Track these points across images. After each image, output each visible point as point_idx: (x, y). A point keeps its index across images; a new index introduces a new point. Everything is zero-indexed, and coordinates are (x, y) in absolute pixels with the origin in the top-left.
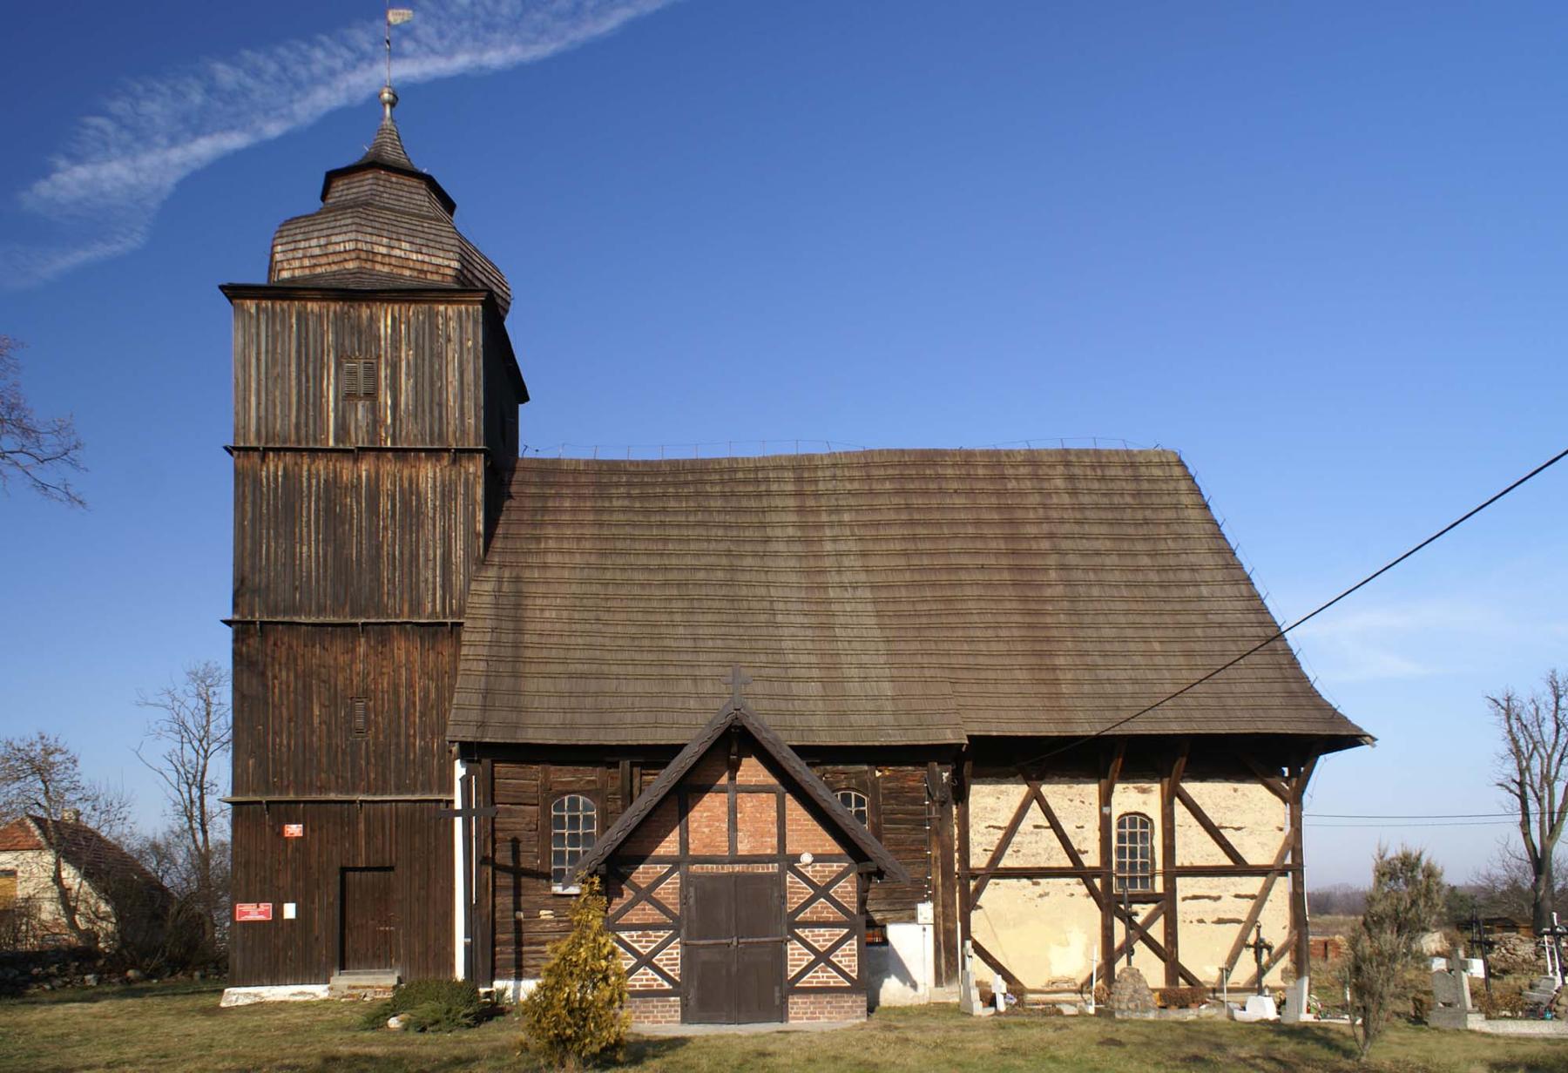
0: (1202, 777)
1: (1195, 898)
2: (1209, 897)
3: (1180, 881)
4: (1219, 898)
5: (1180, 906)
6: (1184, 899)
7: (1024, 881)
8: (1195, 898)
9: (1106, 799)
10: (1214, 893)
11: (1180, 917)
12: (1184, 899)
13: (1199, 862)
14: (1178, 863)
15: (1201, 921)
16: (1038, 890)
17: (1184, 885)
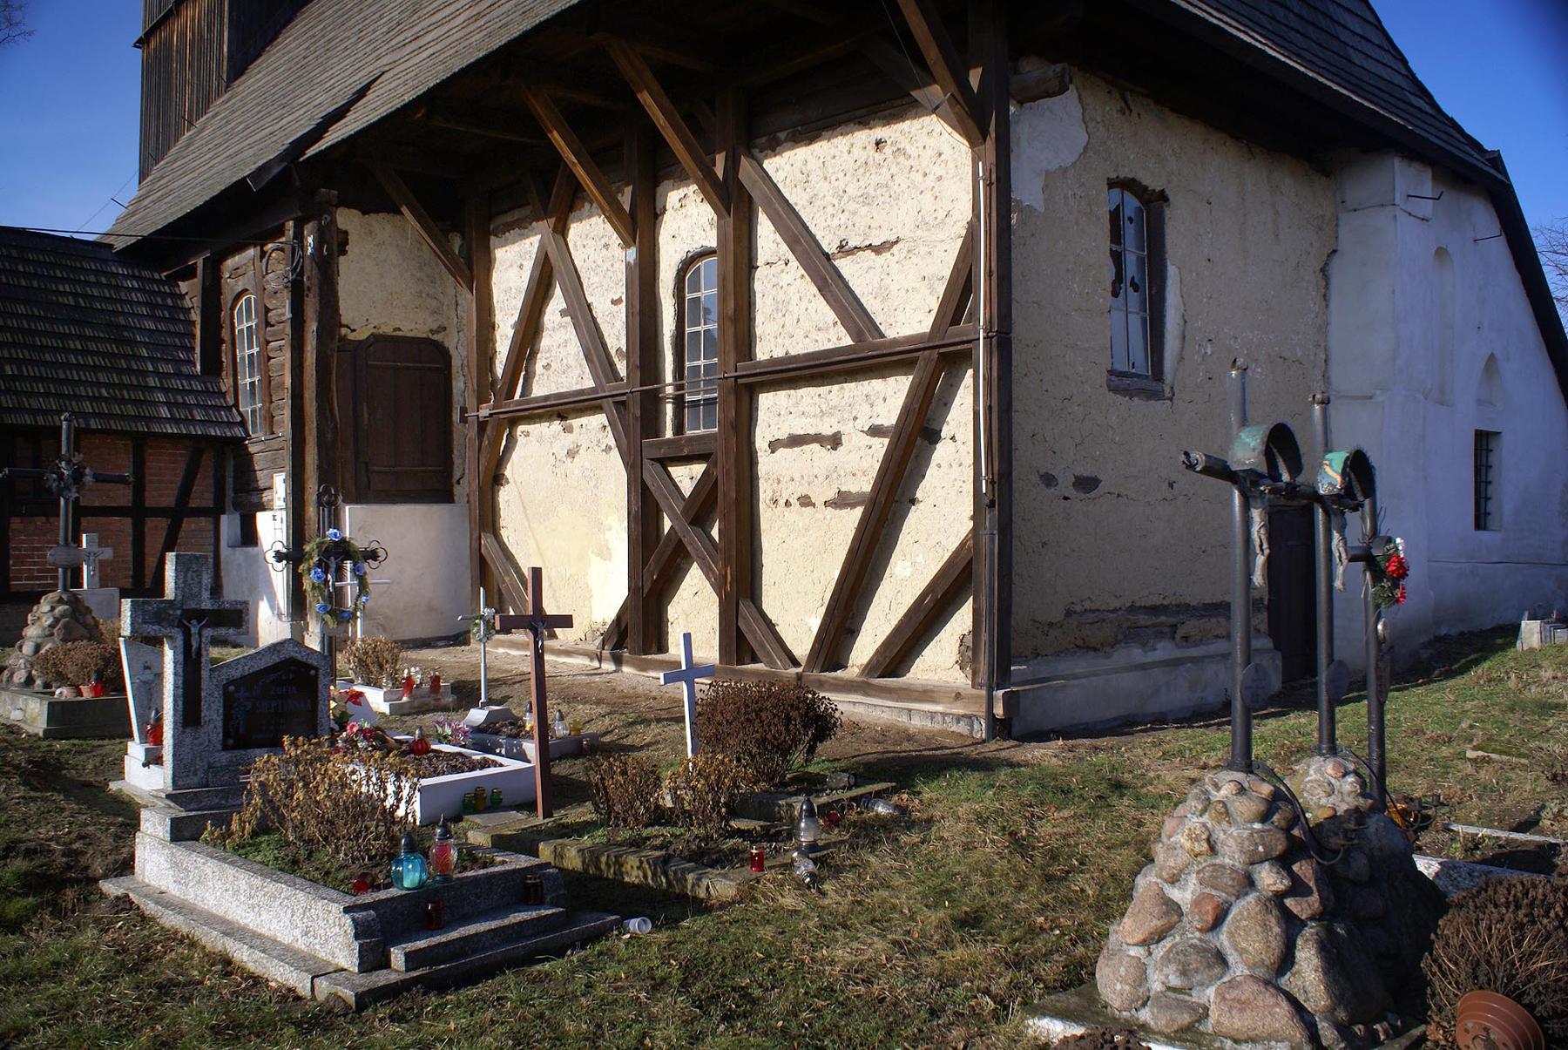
0: (808, 132)
1: (796, 441)
2: (817, 439)
3: (766, 400)
4: (835, 441)
5: (768, 464)
6: (774, 446)
7: (556, 425)
8: (796, 441)
9: (640, 226)
10: (827, 431)
11: (765, 491)
12: (774, 446)
13: (800, 345)
14: (763, 352)
15: (806, 501)
16: (568, 440)
17: (777, 412)
